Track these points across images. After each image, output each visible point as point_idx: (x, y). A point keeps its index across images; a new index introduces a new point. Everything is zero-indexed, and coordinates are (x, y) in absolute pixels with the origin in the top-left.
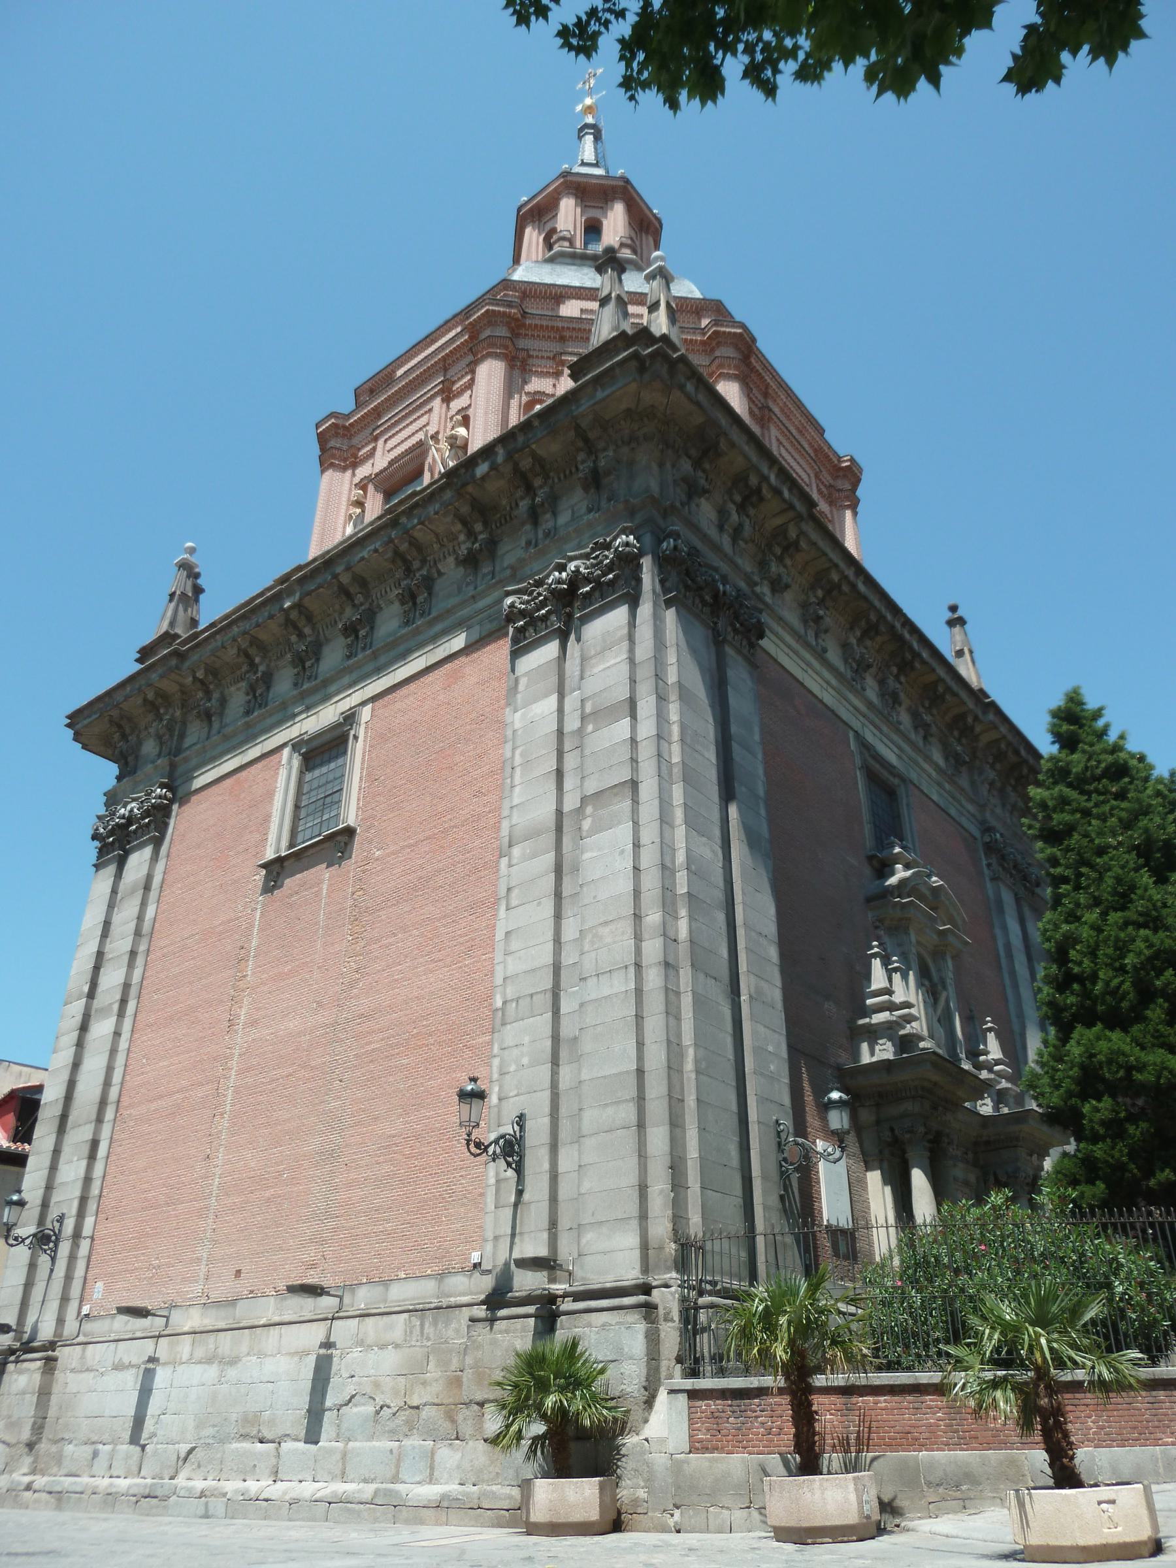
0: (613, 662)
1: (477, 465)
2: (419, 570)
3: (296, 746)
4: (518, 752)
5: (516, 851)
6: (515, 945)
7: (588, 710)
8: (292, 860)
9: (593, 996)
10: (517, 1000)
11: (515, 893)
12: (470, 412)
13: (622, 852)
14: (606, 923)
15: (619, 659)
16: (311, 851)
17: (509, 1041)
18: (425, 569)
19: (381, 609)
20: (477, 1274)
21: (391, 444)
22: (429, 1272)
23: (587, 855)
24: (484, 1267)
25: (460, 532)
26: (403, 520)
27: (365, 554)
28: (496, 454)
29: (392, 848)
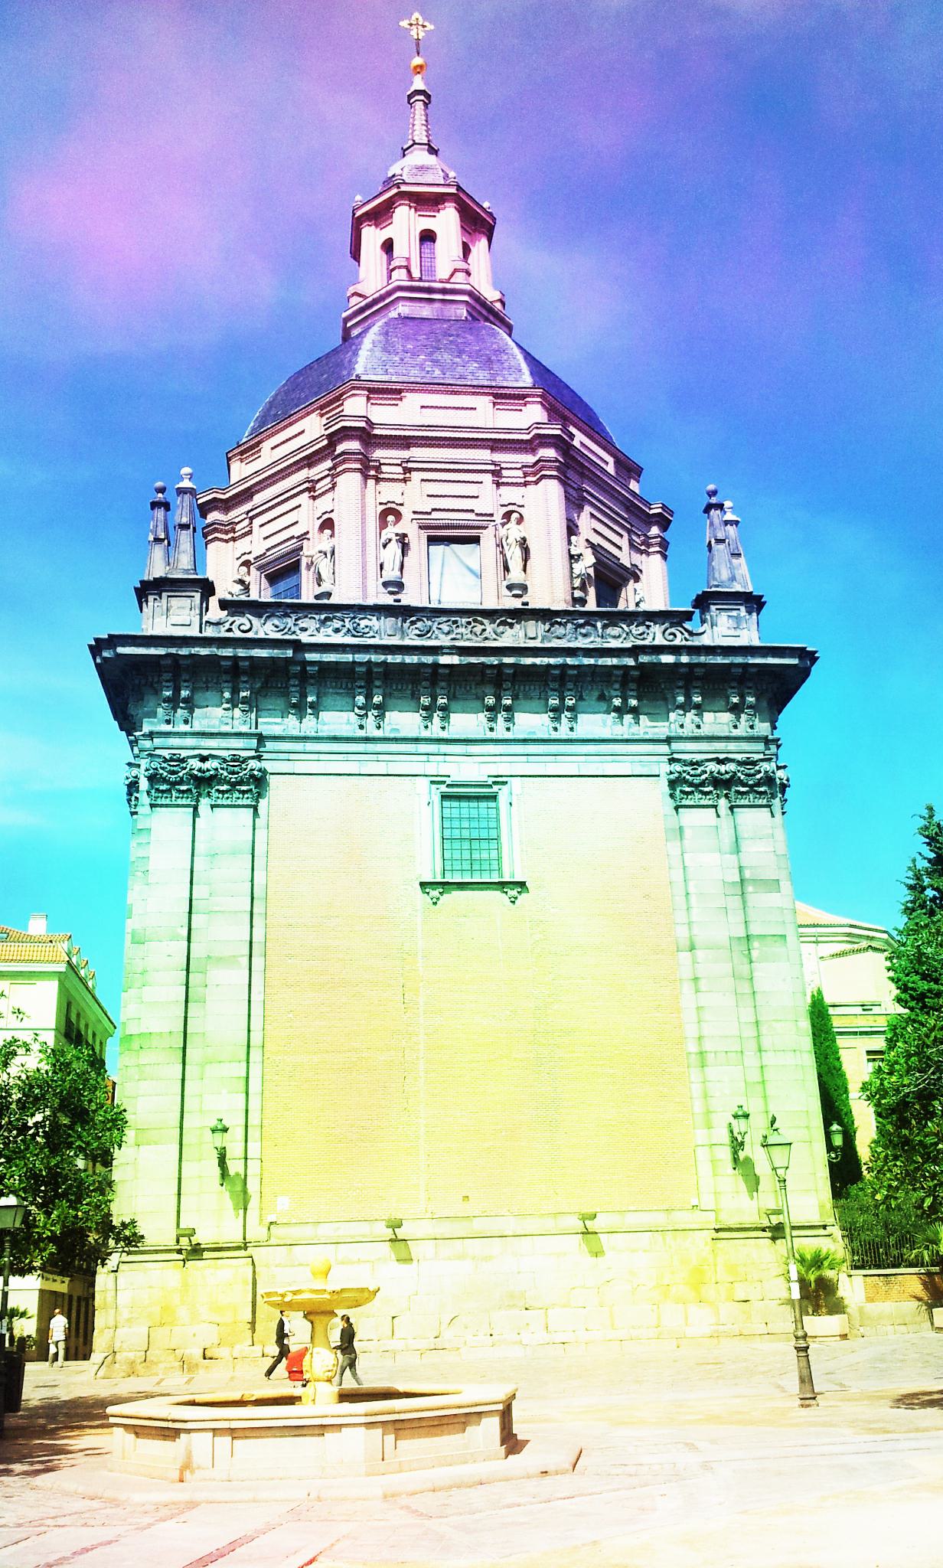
5: (700, 954)
7: (747, 874)
8: (455, 886)
10: (715, 1053)
13: (784, 980)
18: (574, 691)
22: (655, 1208)
25: (616, 682)
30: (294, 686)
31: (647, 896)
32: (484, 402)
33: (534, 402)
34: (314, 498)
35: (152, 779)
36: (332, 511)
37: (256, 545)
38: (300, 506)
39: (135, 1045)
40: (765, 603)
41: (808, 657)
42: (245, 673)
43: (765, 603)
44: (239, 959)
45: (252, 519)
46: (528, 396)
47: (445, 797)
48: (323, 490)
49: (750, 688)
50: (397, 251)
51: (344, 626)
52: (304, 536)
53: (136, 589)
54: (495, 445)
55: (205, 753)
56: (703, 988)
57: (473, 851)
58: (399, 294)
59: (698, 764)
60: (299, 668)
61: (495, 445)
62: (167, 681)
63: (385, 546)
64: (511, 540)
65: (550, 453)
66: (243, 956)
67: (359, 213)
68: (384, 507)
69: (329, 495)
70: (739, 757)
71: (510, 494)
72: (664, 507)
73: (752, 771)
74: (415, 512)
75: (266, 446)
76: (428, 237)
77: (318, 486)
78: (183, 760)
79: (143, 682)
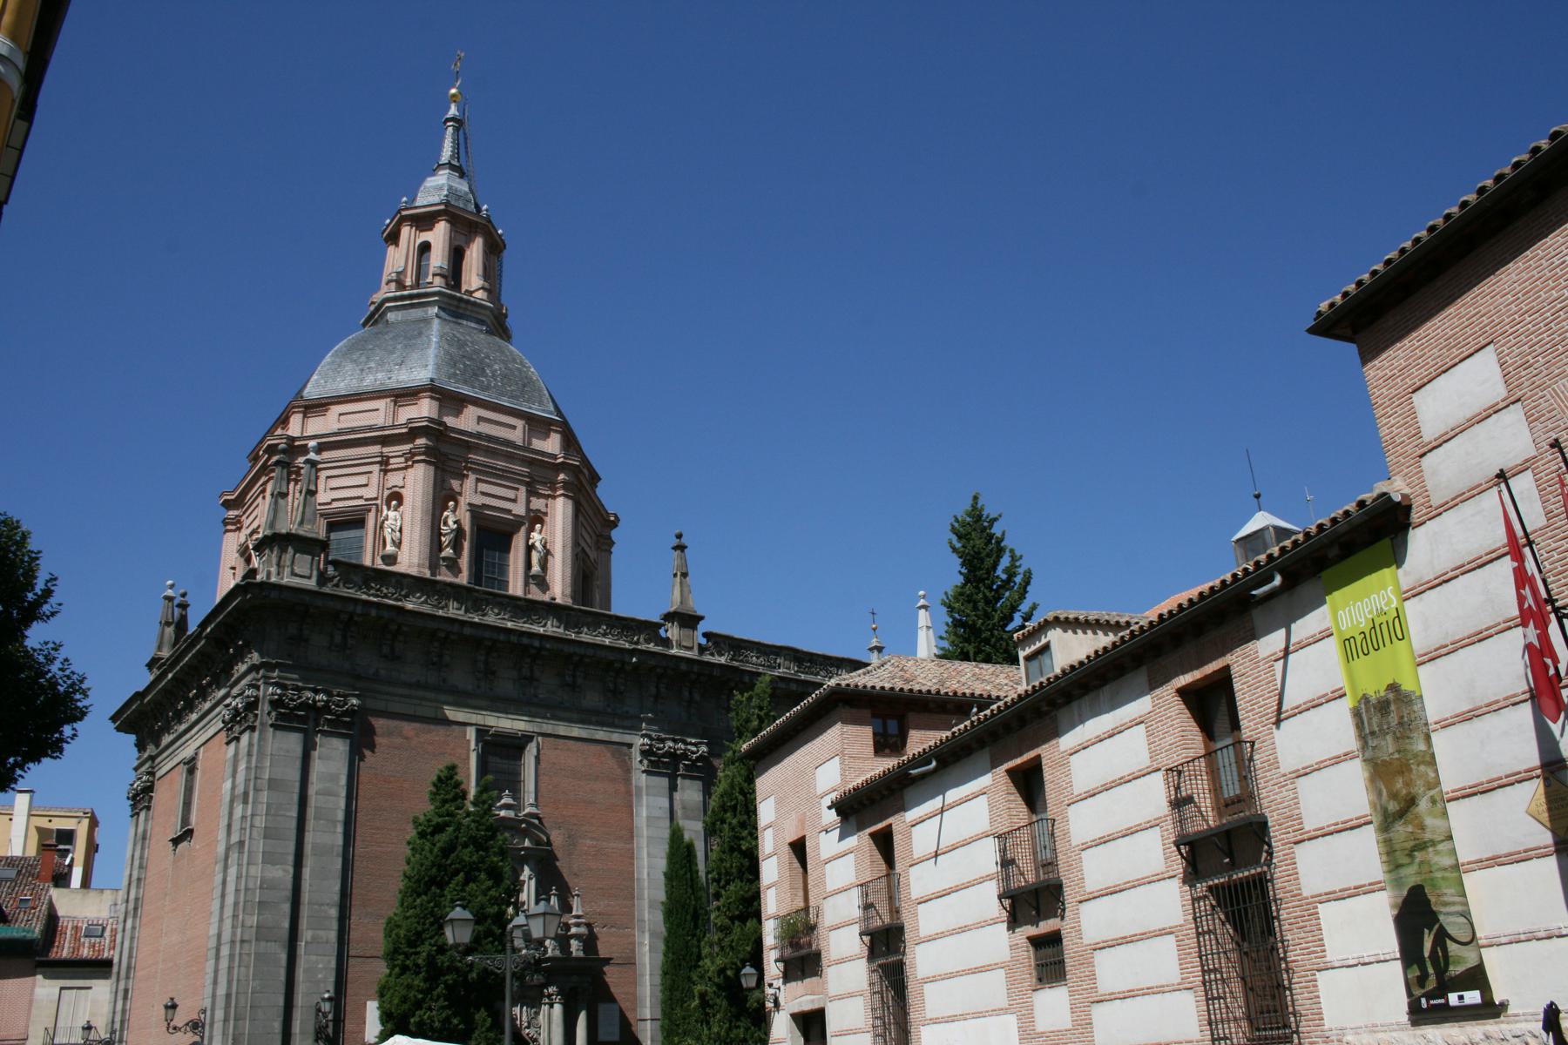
3: (482, 732)
21: (483, 487)
32: (520, 423)
33: (556, 431)
34: (386, 472)
35: (276, 704)
36: (403, 487)
38: (371, 472)
48: (396, 466)
54: (530, 463)
61: (530, 463)
67: (404, 213)
69: (401, 474)
71: (537, 504)
75: (336, 410)
76: (457, 256)
77: (392, 461)
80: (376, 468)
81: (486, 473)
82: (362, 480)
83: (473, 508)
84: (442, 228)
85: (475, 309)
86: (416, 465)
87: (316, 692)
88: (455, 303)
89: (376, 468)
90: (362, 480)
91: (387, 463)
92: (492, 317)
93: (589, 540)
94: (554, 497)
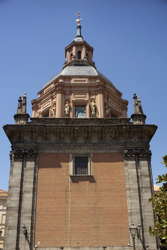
0: (146, 168)
1: (123, 126)
2: (103, 135)
4: (130, 176)
5: (131, 191)
6: (133, 205)
9: (147, 215)
10: (134, 212)
11: (132, 197)
12: (96, 100)
14: (148, 205)
15: (146, 168)
16: (82, 176)
17: (133, 218)
19: (92, 137)
20: (129, 247)
21: (76, 96)
23: (144, 195)
24: (131, 246)
26: (106, 127)
27: (96, 128)
28: (127, 126)
29: (102, 182)
30: (44, 135)
31: (120, 179)
32: (87, 79)
34: (52, 100)
36: (56, 101)
37: (41, 110)
38: (50, 101)
39: (9, 210)
40: (146, 117)
41: (155, 128)
42: (34, 132)
43: (146, 117)
44: (31, 192)
45: (41, 105)
46: (97, 78)
47: (76, 158)
49: (143, 134)
50: (73, 55)
51: (55, 123)
52: (50, 107)
53: (14, 117)
55: (25, 149)
56: (132, 198)
57: (78, 166)
58: (73, 62)
59: (132, 150)
60: (45, 131)
62: (18, 134)
63: (66, 108)
64: (92, 105)
65: (101, 88)
66: (31, 191)
68: (66, 100)
70: (141, 149)
72: (126, 100)
73: (144, 152)
74: (72, 101)
76: (79, 53)
78: (21, 151)
79: (14, 135)
80: (50, 100)
81: (76, 93)
82: (48, 104)
83: (73, 102)
84: (74, 48)
85: (83, 62)
86: (58, 95)
87: (25, 150)
88: (78, 62)
89: (50, 100)
90: (48, 104)
91: (53, 98)
92: (88, 63)
93: (116, 107)
94: (98, 94)
